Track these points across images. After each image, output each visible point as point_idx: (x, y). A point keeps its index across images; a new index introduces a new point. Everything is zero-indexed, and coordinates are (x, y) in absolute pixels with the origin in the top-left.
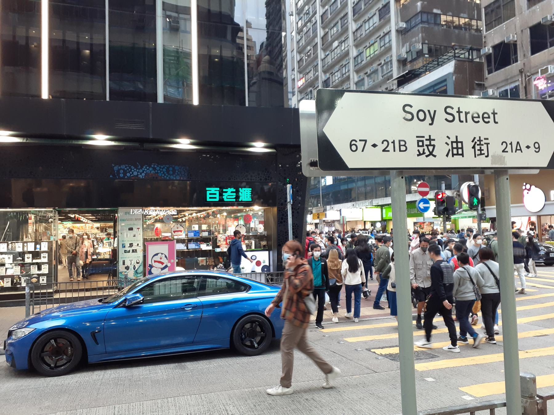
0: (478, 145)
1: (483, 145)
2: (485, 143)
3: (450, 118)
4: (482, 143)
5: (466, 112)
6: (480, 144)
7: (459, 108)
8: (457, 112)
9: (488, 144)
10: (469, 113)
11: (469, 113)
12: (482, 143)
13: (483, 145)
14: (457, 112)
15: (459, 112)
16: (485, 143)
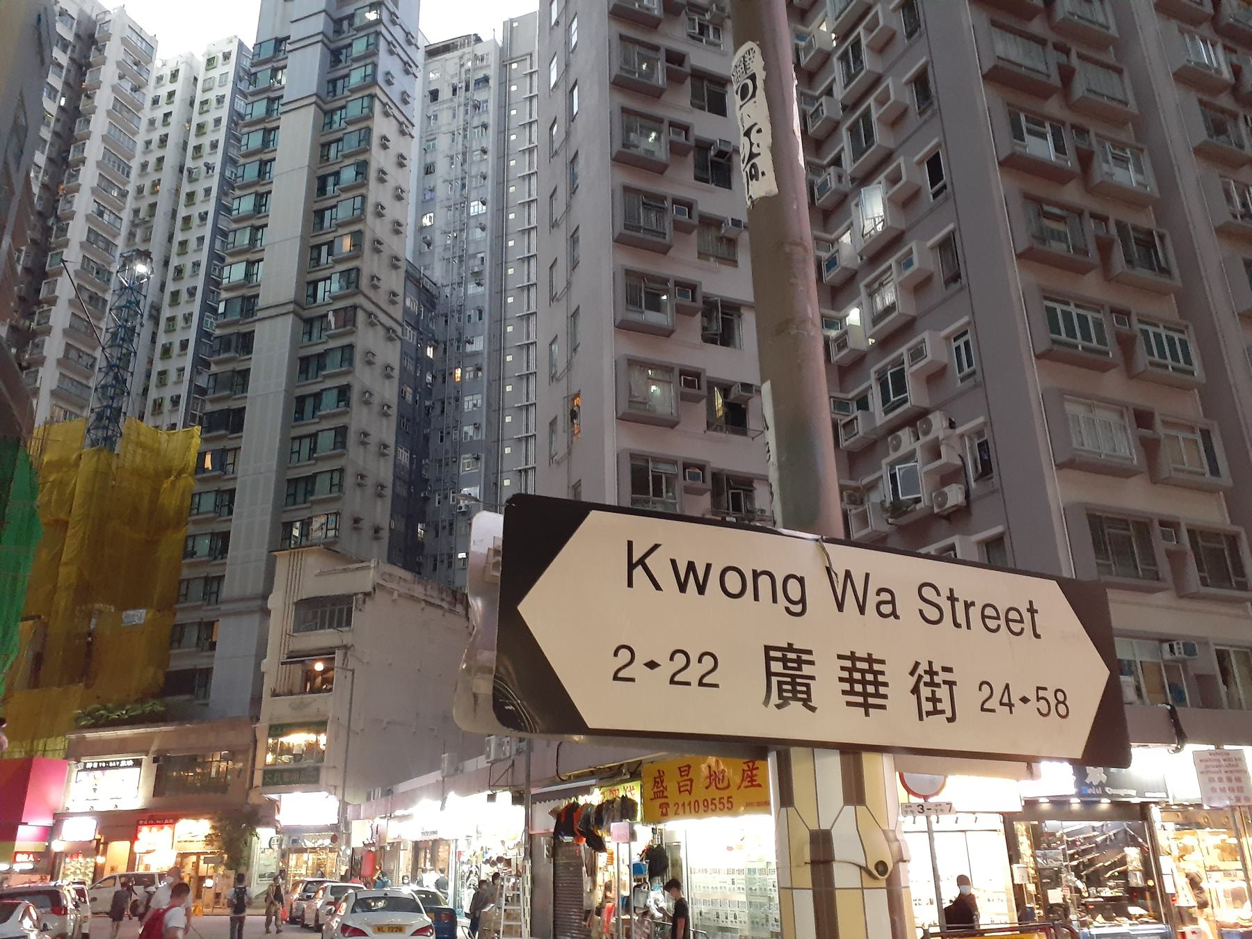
0: (926, 684)
1: (938, 685)
2: (945, 682)
3: (932, 614)
4: (937, 679)
5: (966, 602)
6: (931, 684)
7: (951, 590)
8: (948, 598)
9: (951, 684)
10: (973, 604)
11: (973, 604)
12: (937, 679)
13: (938, 685)
14: (948, 598)
15: (952, 599)
16: (945, 682)
